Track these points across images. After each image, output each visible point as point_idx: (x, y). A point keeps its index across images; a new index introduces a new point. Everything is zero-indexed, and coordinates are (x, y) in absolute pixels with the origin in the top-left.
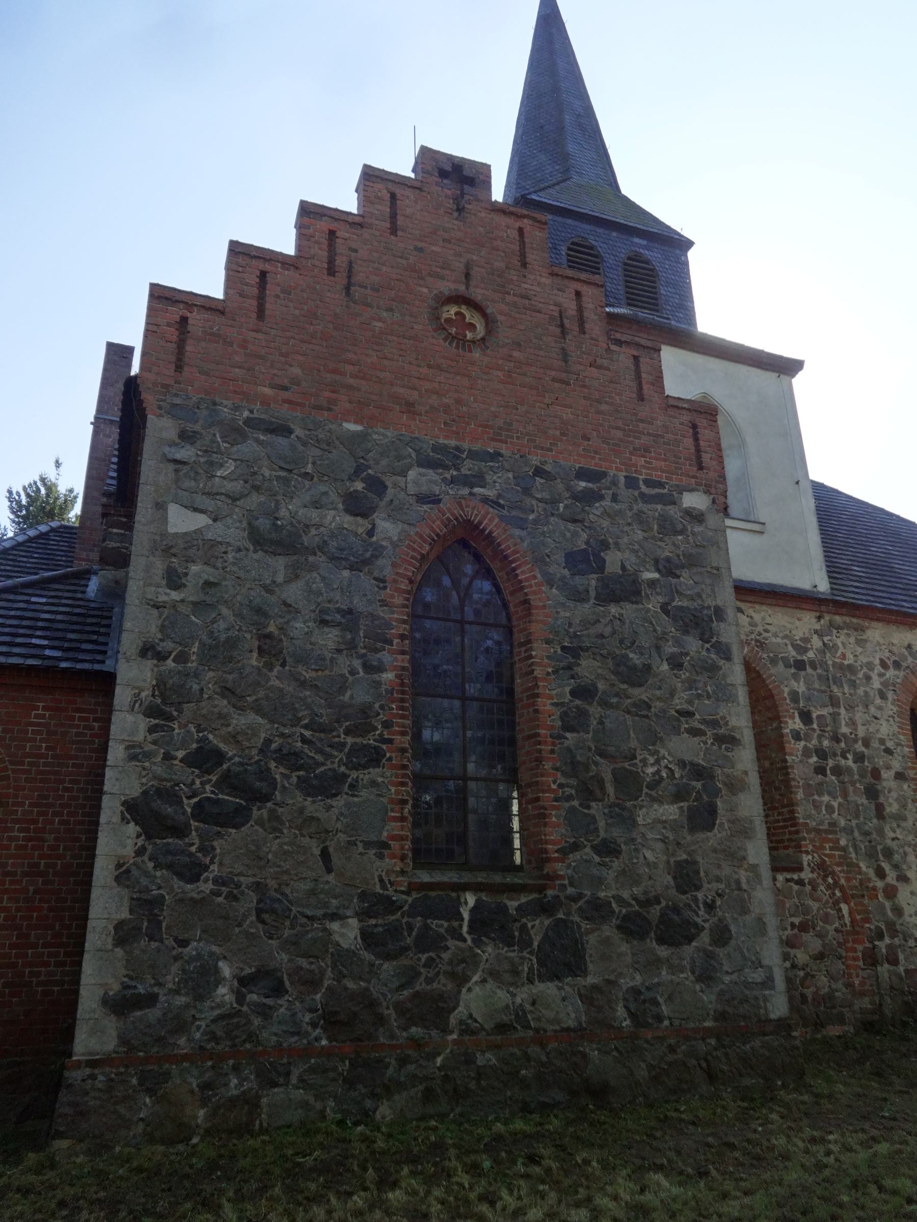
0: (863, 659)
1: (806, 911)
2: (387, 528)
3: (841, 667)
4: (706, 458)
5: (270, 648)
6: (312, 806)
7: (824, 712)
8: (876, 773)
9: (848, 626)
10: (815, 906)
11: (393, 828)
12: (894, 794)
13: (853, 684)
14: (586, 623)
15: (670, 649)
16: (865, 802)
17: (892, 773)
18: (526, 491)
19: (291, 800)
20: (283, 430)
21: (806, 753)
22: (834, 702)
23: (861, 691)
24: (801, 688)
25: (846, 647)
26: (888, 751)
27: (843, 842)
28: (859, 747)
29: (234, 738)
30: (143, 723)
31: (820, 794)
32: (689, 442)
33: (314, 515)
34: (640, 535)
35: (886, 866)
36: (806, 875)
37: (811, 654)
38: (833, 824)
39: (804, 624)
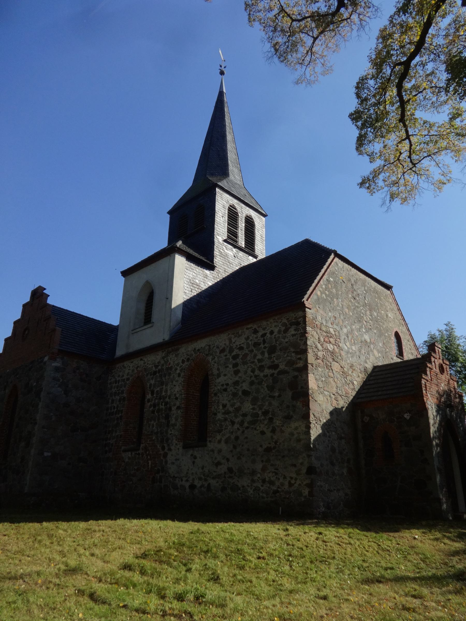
7: (158, 389)
8: (170, 409)
12: (174, 416)
13: (170, 374)
16: (164, 421)
17: (176, 407)
23: (172, 377)
26: (177, 399)
28: (167, 400)
35: (165, 445)
36: (141, 451)
37: (160, 367)
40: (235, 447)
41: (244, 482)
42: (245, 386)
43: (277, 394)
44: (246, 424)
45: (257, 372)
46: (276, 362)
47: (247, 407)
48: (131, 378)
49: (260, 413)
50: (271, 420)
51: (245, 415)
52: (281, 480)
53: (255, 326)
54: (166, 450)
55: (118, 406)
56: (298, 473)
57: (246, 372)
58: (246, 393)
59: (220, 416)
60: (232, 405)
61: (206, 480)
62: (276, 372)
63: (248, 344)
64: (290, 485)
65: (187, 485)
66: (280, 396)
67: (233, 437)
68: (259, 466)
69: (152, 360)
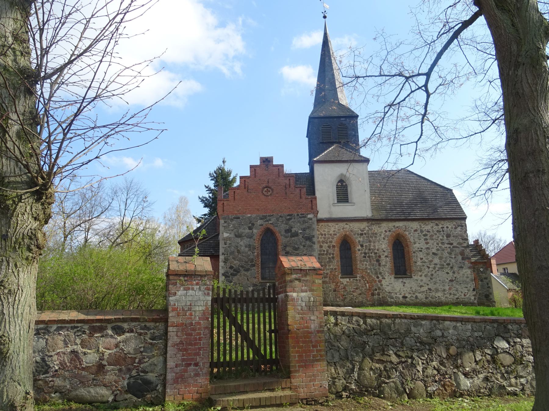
0: (380, 231)
1: (358, 285)
2: (255, 231)
3: (373, 234)
4: (313, 207)
5: (239, 252)
6: (245, 273)
7: (367, 244)
8: (380, 257)
9: (376, 224)
10: (360, 284)
11: (257, 275)
13: (376, 237)
14: (288, 242)
15: (303, 244)
18: (278, 221)
19: (243, 272)
20: (239, 218)
21: (361, 253)
22: (370, 242)
23: (378, 238)
24: (361, 239)
25: (375, 228)
26: (384, 251)
27: (368, 271)
28: (376, 251)
29: (235, 265)
30: (223, 264)
31: (364, 262)
32: (310, 205)
33: (244, 231)
34: (299, 224)
35: (379, 276)
36: (358, 278)
38: (366, 268)
39: (364, 225)
40: (431, 279)
41: (440, 294)
42: (434, 250)
43: (453, 256)
44: (437, 269)
45: (440, 245)
46: (451, 242)
47: (436, 260)
48: (338, 234)
49: (445, 264)
50: (452, 268)
51: (436, 264)
52: (460, 293)
53: (437, 222)
54: (381, 278)
55: (327, 251)
56: (469, 290)
57: (433, 244)
58: (434, 254)
59: (419, 263)
60: (427, 259)
61: (414, 294)
62: (451, 246)
63: (433, 230)
64: (465, 295)
65: (401, 296)
66: (455, 257)
67: (429, 274)
68: (447, 288)
69: (356, 227)
